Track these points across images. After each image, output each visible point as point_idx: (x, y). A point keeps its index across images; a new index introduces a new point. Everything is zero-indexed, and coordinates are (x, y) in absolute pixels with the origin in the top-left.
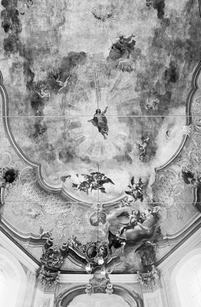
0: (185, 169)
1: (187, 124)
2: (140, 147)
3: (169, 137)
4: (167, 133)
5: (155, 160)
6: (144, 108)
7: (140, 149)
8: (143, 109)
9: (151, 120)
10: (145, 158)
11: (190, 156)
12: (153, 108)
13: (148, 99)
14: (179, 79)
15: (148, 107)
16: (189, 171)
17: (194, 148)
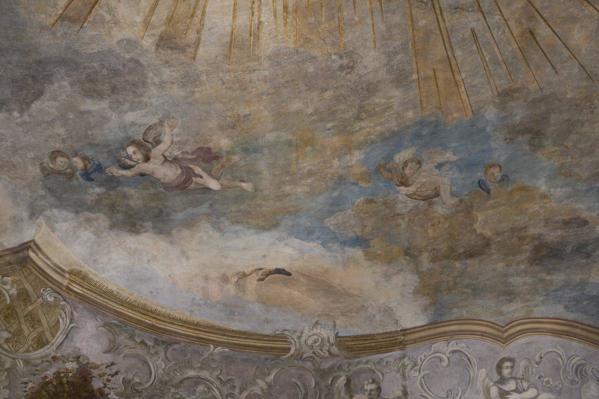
0: (106, 377)
1: (340, 341)
2: (146, 146)
3: (256, 282)
4: (279, 271)
5: (86, 235)
6: (398, 148)
7: (124, 149)
8: (394, 139)
9: (334, 189)
10: (75, 183)
11: (188, 378)
12: (402, 189)
13: (454, 158)
14: (543, 275)
15: (406, 164)
16: (107, 391)
17: (234, 387)
